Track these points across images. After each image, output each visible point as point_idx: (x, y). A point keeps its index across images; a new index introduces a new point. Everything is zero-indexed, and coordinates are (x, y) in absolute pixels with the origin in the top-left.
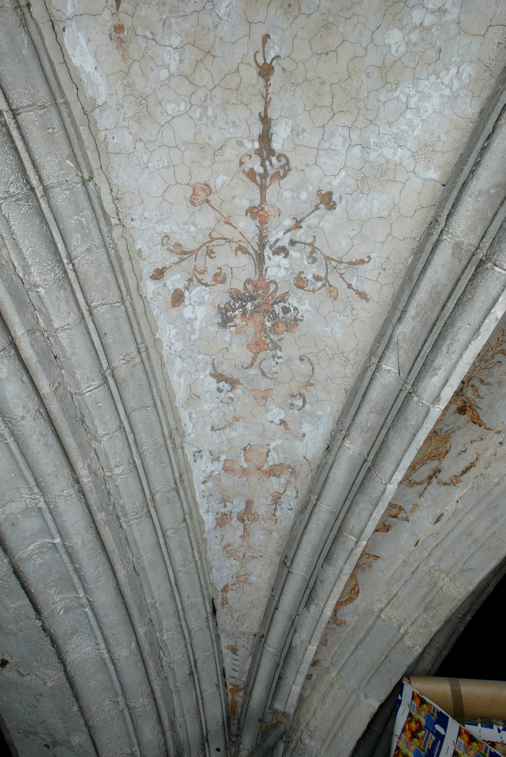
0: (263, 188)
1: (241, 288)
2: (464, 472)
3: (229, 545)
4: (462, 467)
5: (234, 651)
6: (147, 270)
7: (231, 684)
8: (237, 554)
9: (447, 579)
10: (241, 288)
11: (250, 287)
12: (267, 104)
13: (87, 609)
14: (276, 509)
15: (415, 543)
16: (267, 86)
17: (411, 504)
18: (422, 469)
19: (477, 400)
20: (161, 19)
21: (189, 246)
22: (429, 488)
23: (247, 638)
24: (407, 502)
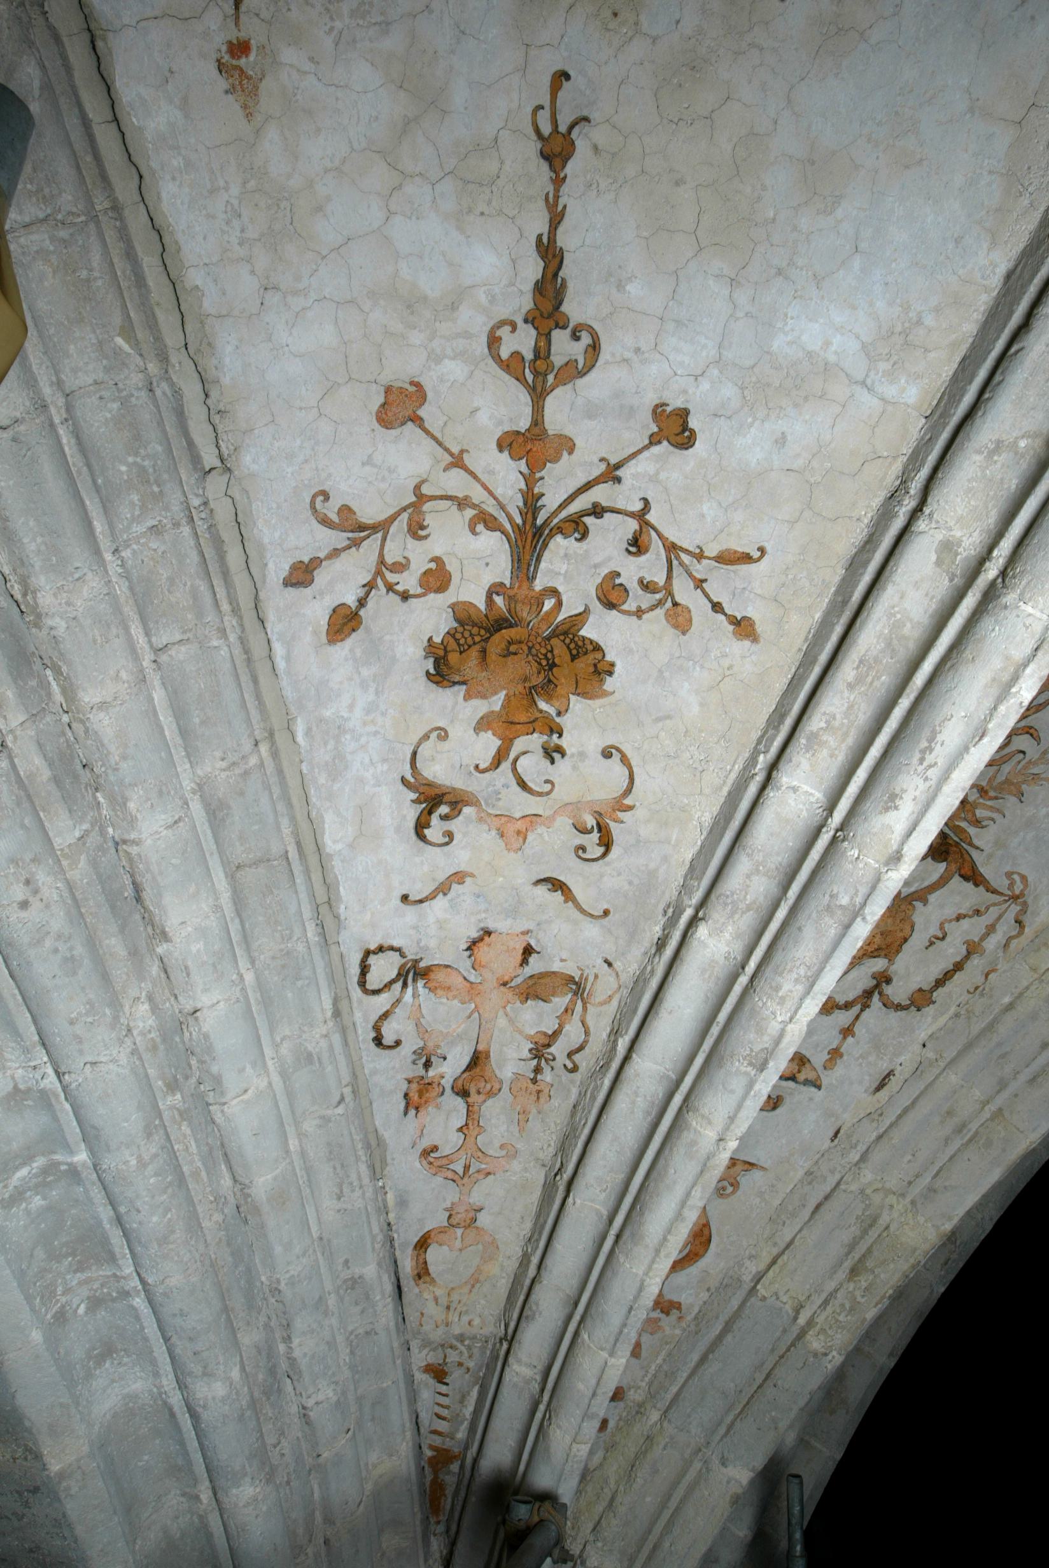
0: (538, 395)
1: (482, 606)
2: (940, 983)
3: (435, 1148)
4: (936, 970)
5: (439, 1373)
6: (277, 568)
7: (431, 1447)
8: (451, 1167)
12: (556, 218)
13: (139, 1302)
14: (538, 1070)
15: (831, 1134)
16: (559, 181)
17: (826, 1052)
19: (972, 831)
20: (332, 29)
21: (369, 513)
23: (469, 1348)
24: (817, 1045)
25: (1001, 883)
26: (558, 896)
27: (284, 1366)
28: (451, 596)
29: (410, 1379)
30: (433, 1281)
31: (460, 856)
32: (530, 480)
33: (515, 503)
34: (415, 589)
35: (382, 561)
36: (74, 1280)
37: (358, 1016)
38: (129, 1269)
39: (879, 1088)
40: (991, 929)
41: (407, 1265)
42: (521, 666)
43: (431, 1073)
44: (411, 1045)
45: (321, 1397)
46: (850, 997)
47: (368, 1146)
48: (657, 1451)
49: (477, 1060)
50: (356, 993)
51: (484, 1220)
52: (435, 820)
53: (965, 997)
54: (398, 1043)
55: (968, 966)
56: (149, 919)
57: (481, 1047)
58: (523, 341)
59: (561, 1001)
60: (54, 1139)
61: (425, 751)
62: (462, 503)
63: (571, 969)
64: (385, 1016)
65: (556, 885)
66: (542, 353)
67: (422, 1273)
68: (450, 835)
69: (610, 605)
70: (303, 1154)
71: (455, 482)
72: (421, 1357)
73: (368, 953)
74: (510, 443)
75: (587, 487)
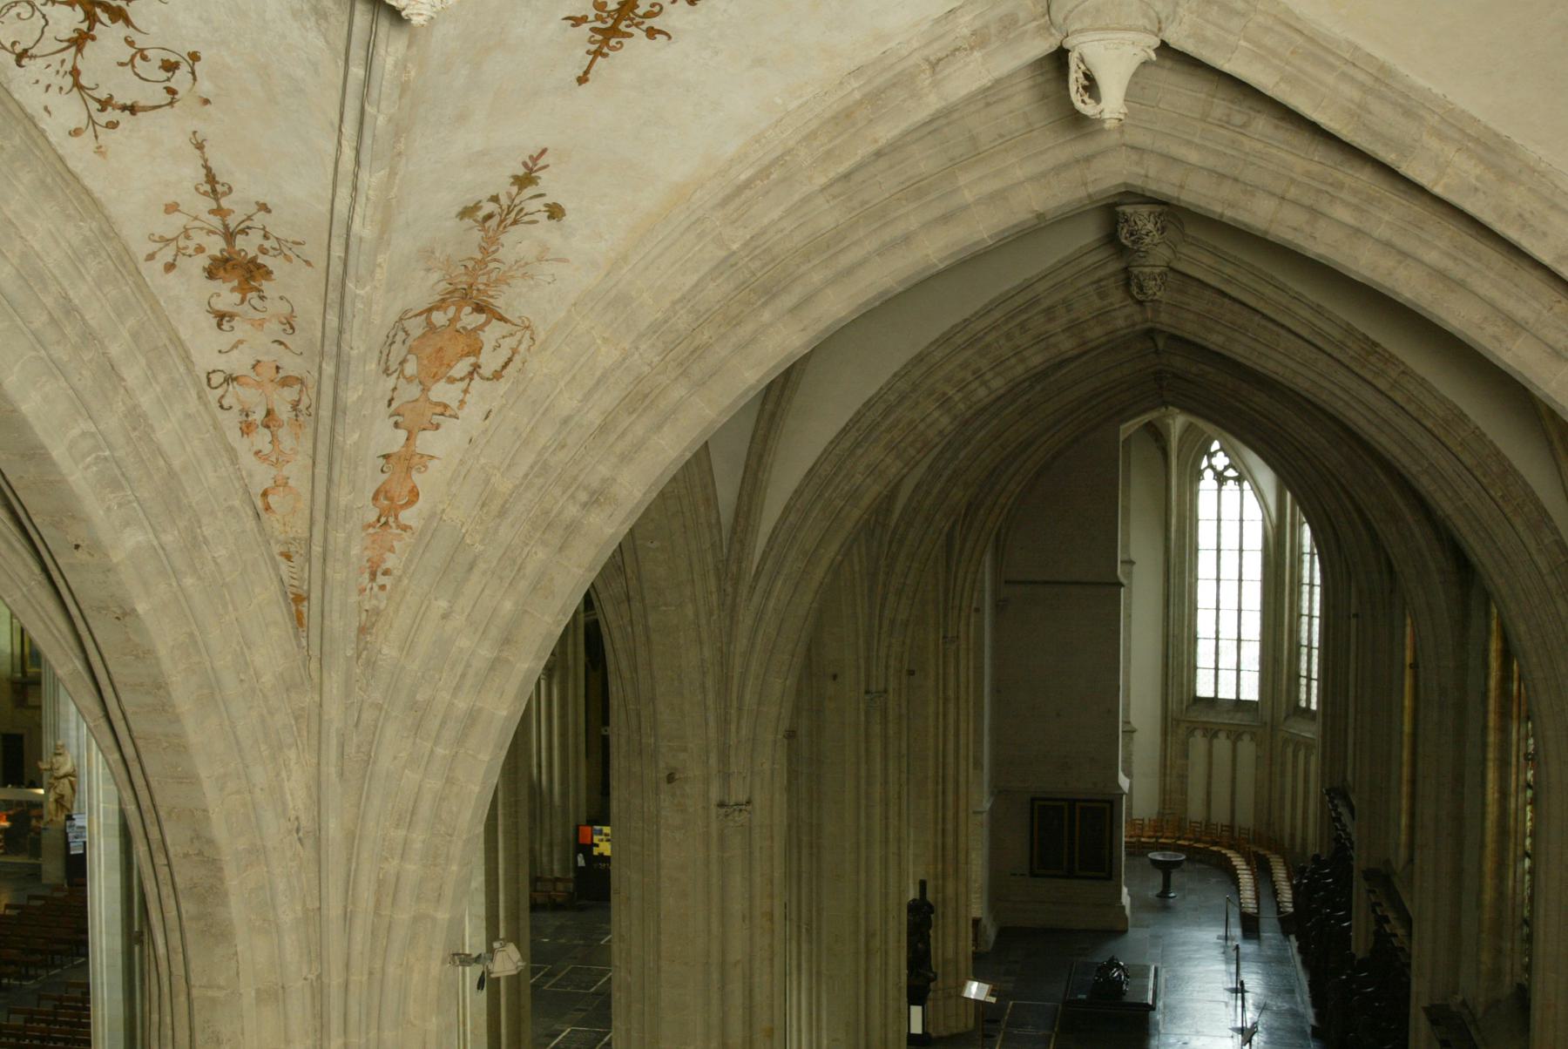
0: (217, 200)
1: (219, 254)
2: (505, 366)
3: (260, 451)
5: (288, 557)
6: (141, 257)
7: (293, 593)
9: (498, 475)
10: (219, 254)
11: (225, 254)
12: (206, 161)
13: (135, 505)
16: (203, 153)
18: (460, 365)
19: (491, 300)
21: (169, 236)
22: (473, 383)
26: (282, 347)
27: (201, 538)
29: (273, 559)
30: (274, 512)
32: (223, 221)
33: (221, 227)
34: (193, 253)
35: (178, 247)
36: (111, 496)
37: (210, 397)
38: (130, 493)
39: (486, 418)
40: (520, 342)
41: (259, 503)
43: (250, 419)
44: (237, 408)
46: (462, 375)
47: (227, 451)
49: (269, 413)
50: (208, 389)
51: (291, 483)
52: (224, 322)
54: (231, 407)
55: (514, 359)
56: (118, 375)
57: (270, 407)
58: (208, 188)
59: (297, 387)
61: (213, 301)
62: (202, 229)
63: (295, 374)
64: (222, 397)
65: (281, 343)
66: (214, 191)
67: (268, 508)
68: (232, 328)
69: (265, 254)
71: (197, 223)
73: (209, 373)
74: (212, 212)
75: (243, 221)
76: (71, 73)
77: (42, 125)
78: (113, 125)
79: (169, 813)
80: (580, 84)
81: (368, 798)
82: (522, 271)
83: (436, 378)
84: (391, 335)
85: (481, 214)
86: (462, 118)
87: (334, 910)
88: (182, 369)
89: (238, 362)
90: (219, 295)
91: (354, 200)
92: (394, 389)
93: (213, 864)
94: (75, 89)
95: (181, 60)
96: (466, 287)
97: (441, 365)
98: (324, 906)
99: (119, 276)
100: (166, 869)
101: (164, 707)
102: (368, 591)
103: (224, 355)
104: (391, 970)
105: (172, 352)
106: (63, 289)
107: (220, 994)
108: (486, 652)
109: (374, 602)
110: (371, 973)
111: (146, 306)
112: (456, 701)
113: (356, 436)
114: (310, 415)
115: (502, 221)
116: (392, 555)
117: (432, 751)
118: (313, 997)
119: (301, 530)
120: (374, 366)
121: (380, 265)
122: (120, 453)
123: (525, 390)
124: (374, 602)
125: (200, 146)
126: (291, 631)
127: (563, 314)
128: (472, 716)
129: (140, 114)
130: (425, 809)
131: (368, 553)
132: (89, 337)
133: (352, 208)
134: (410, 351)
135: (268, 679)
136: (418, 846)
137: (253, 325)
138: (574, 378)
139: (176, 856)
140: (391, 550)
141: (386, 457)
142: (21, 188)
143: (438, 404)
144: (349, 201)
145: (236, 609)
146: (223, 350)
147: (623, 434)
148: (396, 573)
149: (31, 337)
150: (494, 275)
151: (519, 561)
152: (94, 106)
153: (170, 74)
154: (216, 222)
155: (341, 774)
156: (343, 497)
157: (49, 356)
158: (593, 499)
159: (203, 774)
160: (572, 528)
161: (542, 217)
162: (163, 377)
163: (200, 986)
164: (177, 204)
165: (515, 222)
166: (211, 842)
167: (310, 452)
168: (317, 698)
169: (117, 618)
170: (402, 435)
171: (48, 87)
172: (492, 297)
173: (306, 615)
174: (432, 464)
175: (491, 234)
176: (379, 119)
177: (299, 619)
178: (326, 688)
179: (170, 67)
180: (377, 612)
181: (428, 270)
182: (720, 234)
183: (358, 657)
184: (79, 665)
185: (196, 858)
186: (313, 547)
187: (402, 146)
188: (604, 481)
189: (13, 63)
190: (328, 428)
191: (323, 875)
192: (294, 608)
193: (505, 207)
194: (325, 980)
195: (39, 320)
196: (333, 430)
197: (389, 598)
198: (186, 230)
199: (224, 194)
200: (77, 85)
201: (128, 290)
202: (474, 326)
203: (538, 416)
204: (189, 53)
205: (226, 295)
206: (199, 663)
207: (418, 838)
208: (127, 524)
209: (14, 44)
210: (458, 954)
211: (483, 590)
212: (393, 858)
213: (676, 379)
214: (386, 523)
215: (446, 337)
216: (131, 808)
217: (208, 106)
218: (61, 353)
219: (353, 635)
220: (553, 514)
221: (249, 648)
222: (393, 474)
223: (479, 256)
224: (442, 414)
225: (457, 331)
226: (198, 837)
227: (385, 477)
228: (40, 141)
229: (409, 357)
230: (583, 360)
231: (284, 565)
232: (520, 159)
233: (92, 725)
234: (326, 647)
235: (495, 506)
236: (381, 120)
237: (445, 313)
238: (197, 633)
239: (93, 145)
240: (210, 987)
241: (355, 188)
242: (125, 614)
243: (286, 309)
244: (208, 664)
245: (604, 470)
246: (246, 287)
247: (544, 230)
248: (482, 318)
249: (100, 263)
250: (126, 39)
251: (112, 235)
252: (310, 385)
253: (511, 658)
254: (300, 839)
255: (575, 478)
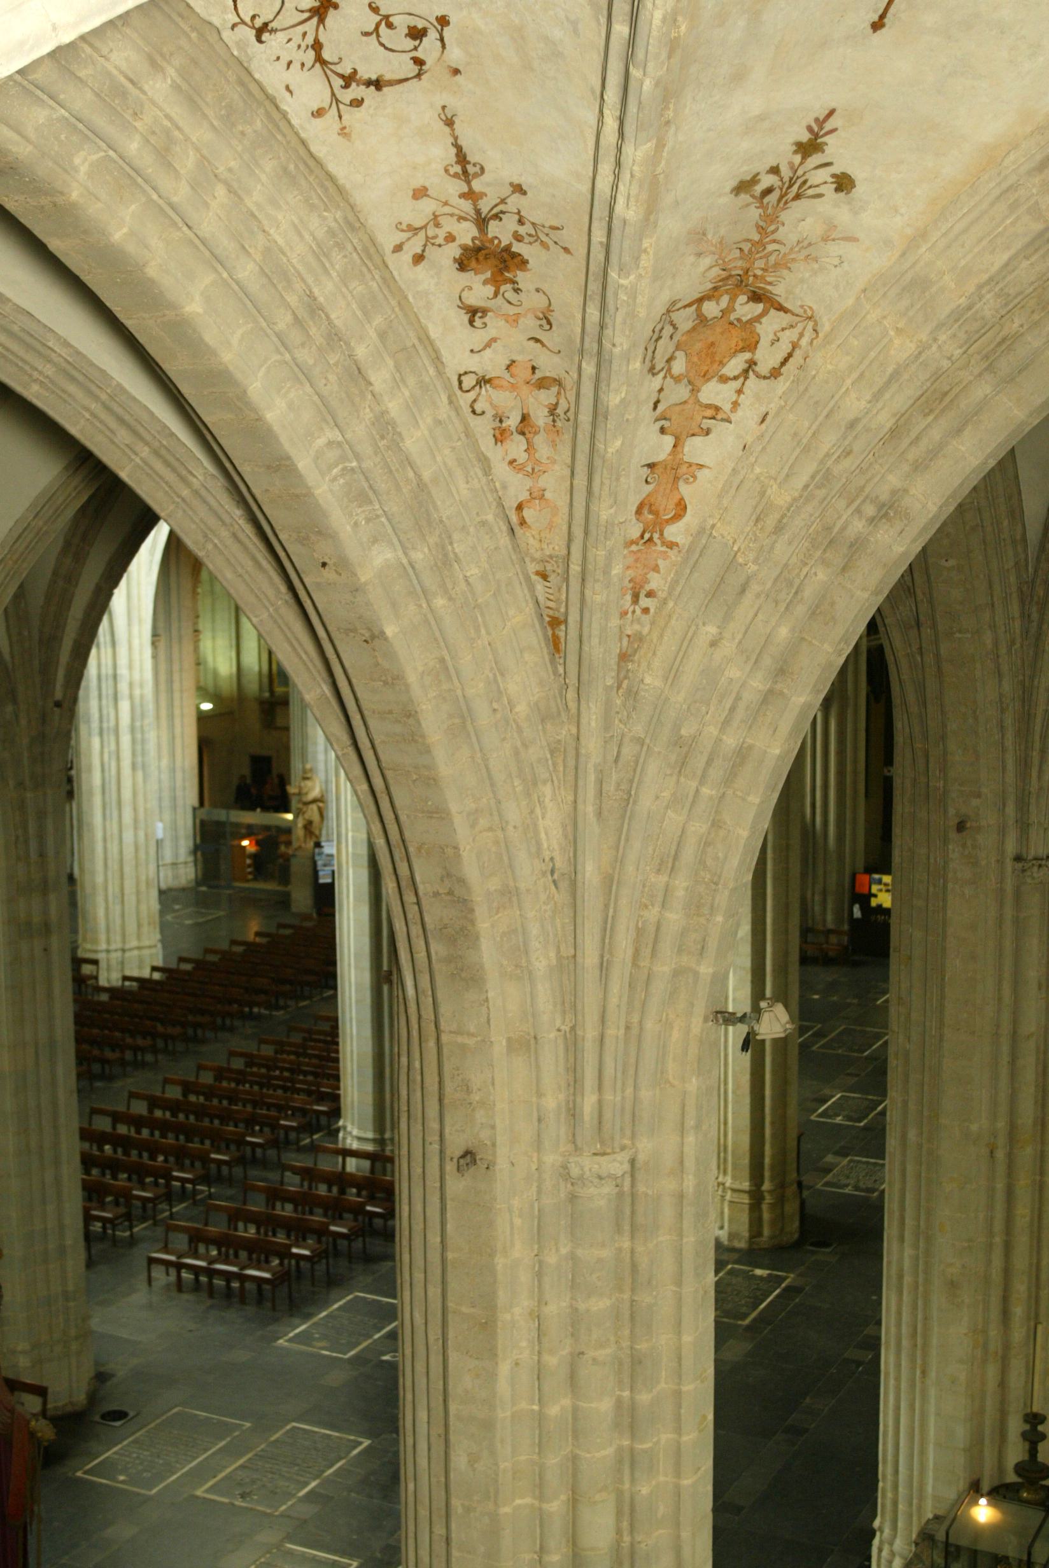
0: (468, 183)
1: (470, 243)
3: (515, 461)
4: (780, 357)
5: (544, 576)
6: (388, 248)
7: (549, 616)
9: (775, 487)
10: (470, 243)
11: (477, 242)
12: (456, 138)
13: (383, 519)
16: (453, 130)
18: (733, 362)
19: (769, 287)
21: (418, 224)
22: (747, 382)
25: (800, 311)
26: (539, 345)
27: (451, 555)
28: (458, 242)
29: (528, 579)
30: (529, 527)
31: (491, 332)
32: (475, 205)
33: (472, 212)
35: (427, 237)
36: (360, 510)
37: (462, 403)
38: (377, 507)
39: (763, 421)
40: (801, 335)
41: (514, 519)
42: (493, 261)
43: (504, 425)
44: (490, 413)
45: (472, 572)
46: (736, 373)
47: (480, 460)
48: (673, 622)
49: (524, 418)
50: (459, 393)
51: (548, 495)
52: (476, 318)
53: (797, 371)
54: (483, 413)
56: (365, 379)
58: (458, 169)
59: (555, 389)
60: (343, 458)
61: (464, 295)
62: (452, 215)
65: (537, 340)
66: (465, 172)
67: (523, 523)
68: (485, 324)
69: (519, 241)
70: (445, 464)
71: (447, 209)
72: (532, 567)
73: (460, 375)
74: (463, 196)
75: (496, 205)
76: (313, 47)
77: (284, 107)
78: (357, 103)
79: (419, 849)
80: (875, 31)
81: (627, 840)
82: (805, 253)
83: (706, 377)
84: (657, 330)
85: (759, 189)
86: (739, 77)
87: (590, 958)
88: (432, 371)
89: (492, 363)
90: (470, 288)
91: (617, 177)
92: (661, 390)
93: (464, 905)
94: (318, 65)
95: (427, 25)
96: (740, 272)
97: (712, 363)
98: (579, 954)
99: (364, 269)
100: (416, 907)
101: (414, 737)
102: (630, 614)
103: (476, 356)
104: (650, 1025)
105: (421, 352)
106: (308, 286)
107: (471, 1042)
108: (758, 684)
109: (637, 627)
110: (628, 1028)
111: (394, 303)
112: (724, 737)
113: (618, 443)
114: (568, 420)
115: (782, 197)
116: (656, 575)
117: (697, 791)
118: (567, 1050)
119: (559, 547)
120: (638, 365)
121: (645, 251)
122: (367, 464)
123: (806, 389)
124: (637, 627)
125: (450, 123)
126: (547, 658)
127: (850, 302)
128: (742, 754)
129: (385, 89)
130: (689, 853)
131: (630, 573)
132: (334, 338)
133: (615, 187)
134: (678, 348)
135: (522, 708)
136: (680, 893)
137: (507, 321)
138: (862, 375)
139: (425, 894)
140: (656, 569)
141: (651, 466)
142: (263, 177)
143: (708, 406)
144: (611, 178)
145: (488, 633)
146: (476, 349)
147: (918, 439)
148: (661, 595)
149: (275, 339)
150: (772, 259)
151: (797, 582)
152: (338, 82)
153: (417, 43)
154: (467, 206)
155: (599, 814)
156: (604, 512)
157: (294, 359)
158: (883, 512)
159: (454, 807)
160: (857, 546)
161: (829, 189)
162: (411, 381)
163: (451, 1032)
164: (425, 189)
165: (798, 197)
166: (462, 881)
167: (569, 461)
168: (574, 731)
169: (366, 641)
170: (669, 440)
171: (289, 63)
172: (770, 283)
173: (562, 640)
174: (703, 475)
175: (770, 211)
176: (646, 84)
177: (555, 645)
178: (584, 721)
179: (416, 34)
180: (640, 638)
181: (699, 255)
182: (1037, 203)
183: (619, 687)
184: (327, 690)
185: (448, 898)
186: (571, 566)
187: (670, 114)
188: (894, 492)
189: (253, 39)
190: (588, 436)
191: (579, 921)
192: (550, 633)
193: (786, 179)
194: (580, 1033)
195: (283, 321)
196: (593, 436)
197: (653, 623)
198: (435, 217)
199: (476, 175)
200: (319, 59)
201: (375, 285)
202: (749, 317)
203: (821, 418)
204: (437, 18)
205: (478, 289)
206: (450, 690)
207: (681, 884)
208: (375, 540)
209: (253, 17)
210: (721, 1012)
211: (756, 615)
212: (653, 905)
213: (980, 375)
214: (650, 540)
215: (719, 330)
216: (380, 842)
217: (458, 77)
218: (305, 356)
219: (613, 661)
220: (836, 530)
221: (502, 675)
222: (658, 485)
223: (756, 237)
224: (713, 418)
225: (731, 323)
226: (449, 875)
227: (650, 488)
228: (282, 124)
229: (678, 354)
230: (873, 354)
231: (540, 586)
232: (804, 124)
233: (340, 753)
234: (585, 677)
235: (770, 522)
236: (648, 84)
237: (718, 303)
238: (447, 658)
239: (337, 126)
240: (458, 1032)
241: (618, 163)
242: (373, 637)
243: (542, 302)
244: (459, 692)
245: (894, 480)
246: (500, 278)
247: (830, 205)
248: (760, 307)
249: (345, 256)
250: (370, 5)
251: (357, 225)
252: (568, 387)
253: (785, 691)
254: (554, 881)
255: (862, 488)
